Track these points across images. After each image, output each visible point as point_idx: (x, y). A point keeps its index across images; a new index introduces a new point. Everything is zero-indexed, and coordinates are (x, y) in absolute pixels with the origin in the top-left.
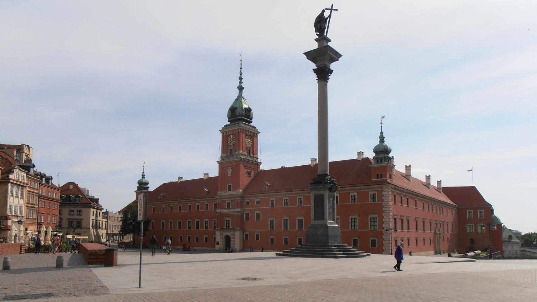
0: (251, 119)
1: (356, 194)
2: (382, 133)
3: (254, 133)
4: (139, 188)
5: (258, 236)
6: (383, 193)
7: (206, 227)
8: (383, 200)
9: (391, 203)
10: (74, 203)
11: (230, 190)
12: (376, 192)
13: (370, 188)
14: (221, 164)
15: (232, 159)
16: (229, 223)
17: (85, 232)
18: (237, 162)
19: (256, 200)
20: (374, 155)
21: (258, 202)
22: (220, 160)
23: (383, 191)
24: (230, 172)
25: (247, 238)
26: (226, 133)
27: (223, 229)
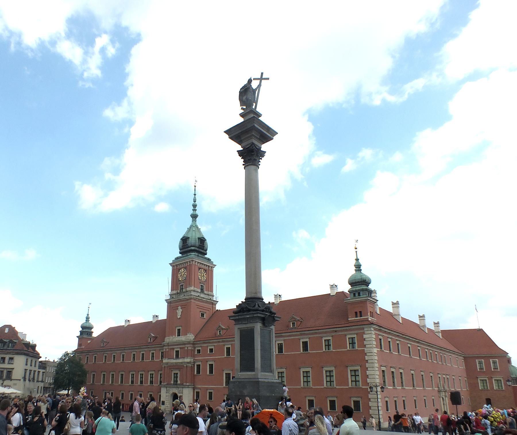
2: (357, 260)
3: (209, 266)
4: (81, 332)
5: (211, 394)
6: (365, 336)
7: (151, 382)
9: (375, 350)
10: (6, 349)
11: (179, 335)
12: (355, 336)
13: (346, 330)
14: (169, 302)
15: (182, 297)
16: (177, 377)
17: (15, 384)
18: (188, 300)
19: (209, 348)
20: (349, 287)
21: (211, 350)
22: (169, 298)
24: (179, 312)
25: (198, 396)
26: (176, 267)
27: (171, 384)
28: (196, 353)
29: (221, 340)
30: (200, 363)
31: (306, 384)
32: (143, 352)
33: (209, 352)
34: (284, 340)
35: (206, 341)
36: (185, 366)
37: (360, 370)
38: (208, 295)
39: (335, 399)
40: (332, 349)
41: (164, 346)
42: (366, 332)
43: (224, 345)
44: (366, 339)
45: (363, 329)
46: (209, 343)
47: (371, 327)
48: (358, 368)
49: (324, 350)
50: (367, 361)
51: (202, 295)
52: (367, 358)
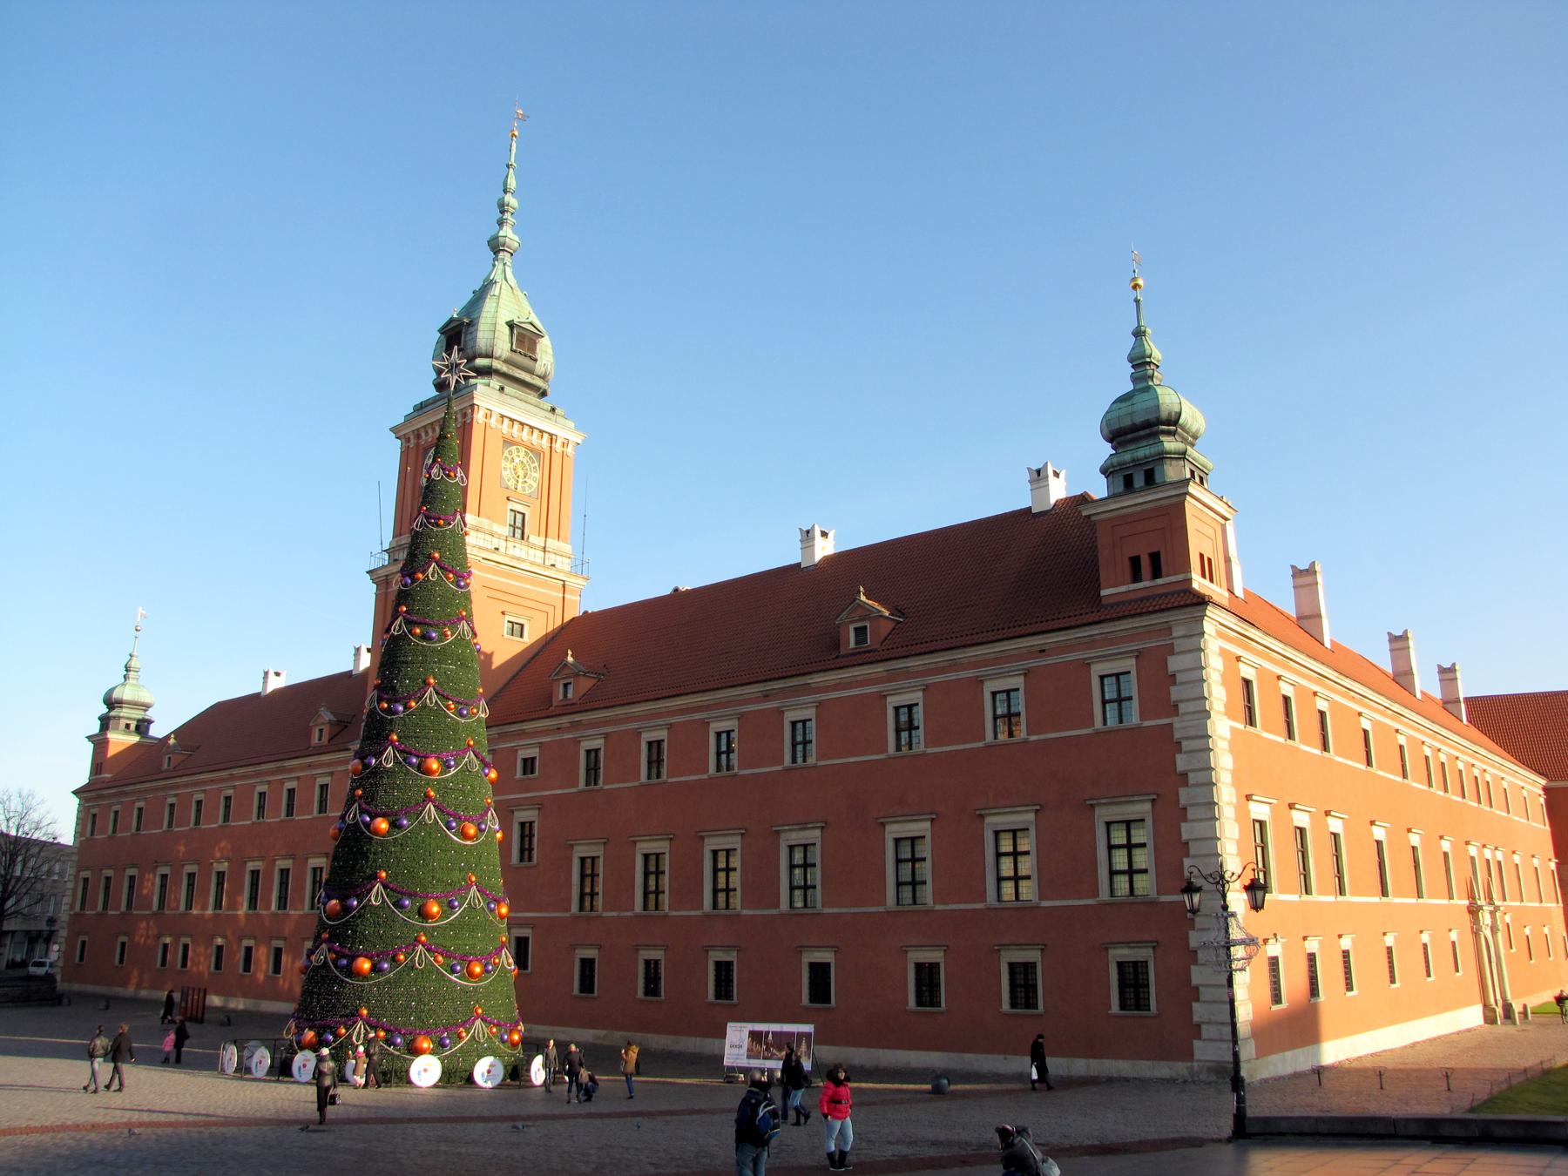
8: (1174, 709)
13: (1092, 643)
21: (529, 765)
23: (1171, 650)
29: (565, 720)
31: (907, 892)
32: (289, 785)
33: (519, 775)
37: (1149, 822)
39: (1032, 955)
40: (1021, 733)
42: (1180, 645)
43: (576, 742)
44: (1179, 678)
45: (1170, 629)
46: (523, 734)
48: (1143, 808)
50: (1184, 775)
51: (518, 550)
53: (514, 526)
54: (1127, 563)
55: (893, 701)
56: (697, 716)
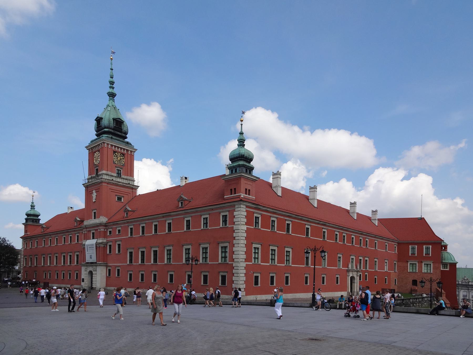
0: (126, 133)
1: (208, 216)
13: (221, 208)
23: (234, 211)
25: (109, 274)
28: (108, 234)
29: (125, 221)
30: (110, 243)
33: (117, 233)
34: (173, 219)
35: (115, 223)
36: (98, 246)
38: (127, 179)
41: (84, 228)
42: (236, 210)
44: (236, 217)
45: (234, 206)
47: (241, 204)
49: (202, 228)
50: (235, 237)
52: (235, 235)
53: (118, 173)
54: (230, 191)
55: (186, 219)
56: (151, 221)
